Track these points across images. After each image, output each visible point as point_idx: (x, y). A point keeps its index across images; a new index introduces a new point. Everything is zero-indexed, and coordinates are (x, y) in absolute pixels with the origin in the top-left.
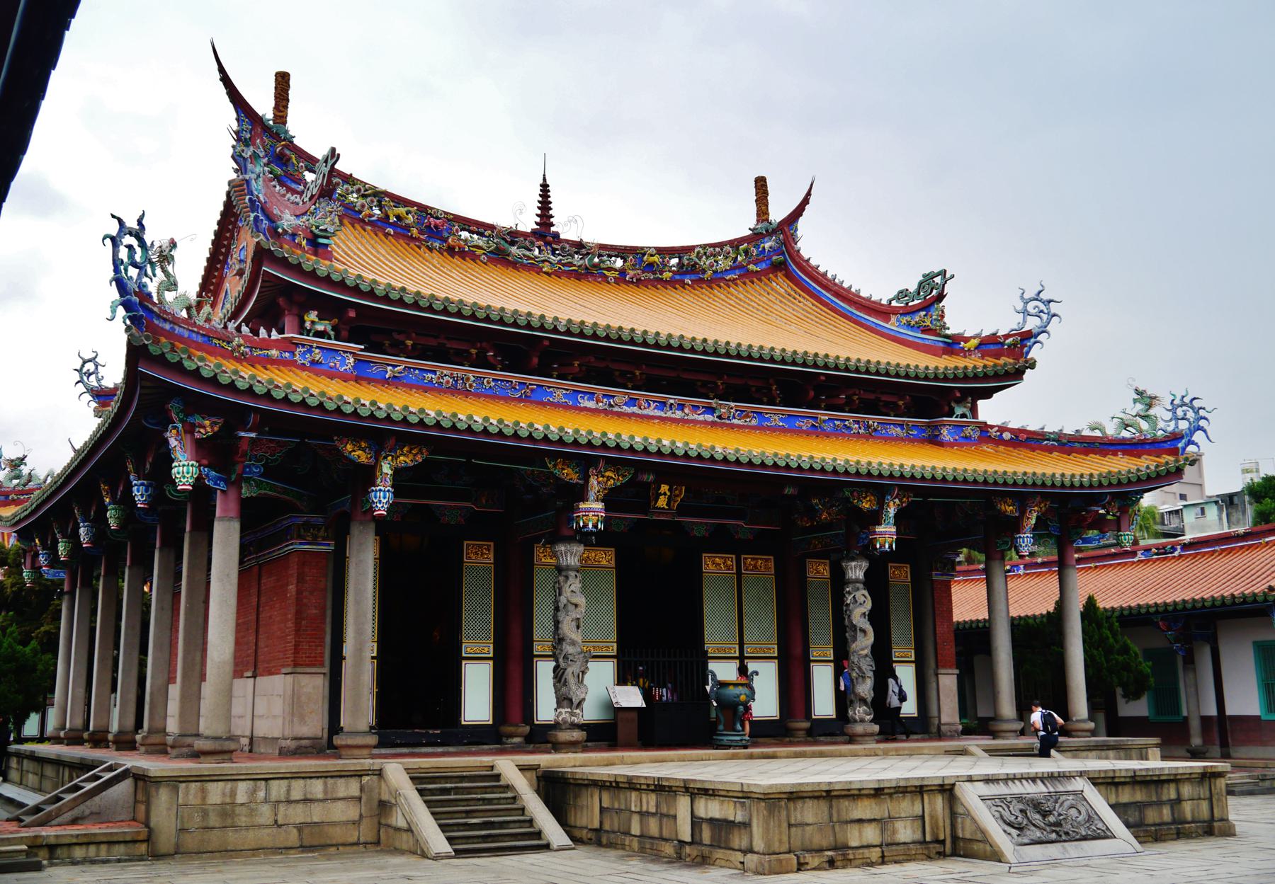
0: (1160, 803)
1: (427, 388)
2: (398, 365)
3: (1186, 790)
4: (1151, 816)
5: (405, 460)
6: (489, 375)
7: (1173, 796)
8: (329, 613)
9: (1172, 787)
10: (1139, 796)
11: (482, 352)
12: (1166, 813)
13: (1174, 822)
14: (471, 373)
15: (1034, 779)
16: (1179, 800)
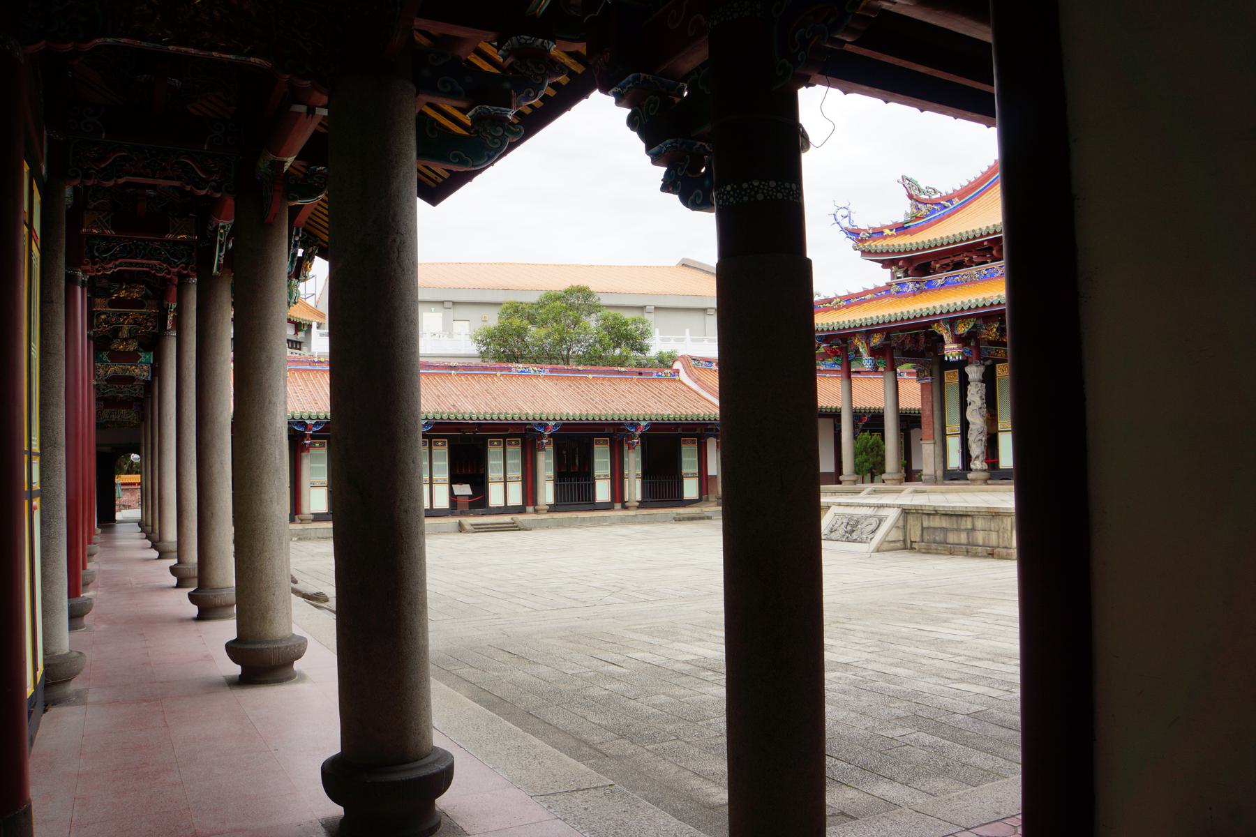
0: (958, 530)
1: (957, 285)
2: (938, 279)
3: (980, 523)
4: (952, 538)
5: (876, 340)
6: (983, 268)
7: (969, 526)
8: (937, 413)
9: (969, 519)
10: (944, 523)
11: (971, 260)
12: (963, 538)
13: (968, 544)
14: (973, 270)
15: (870, 506)
16: (973, 529)
